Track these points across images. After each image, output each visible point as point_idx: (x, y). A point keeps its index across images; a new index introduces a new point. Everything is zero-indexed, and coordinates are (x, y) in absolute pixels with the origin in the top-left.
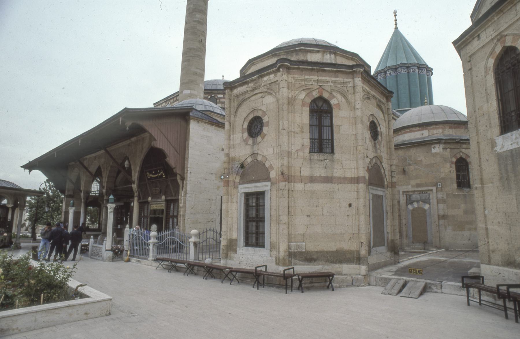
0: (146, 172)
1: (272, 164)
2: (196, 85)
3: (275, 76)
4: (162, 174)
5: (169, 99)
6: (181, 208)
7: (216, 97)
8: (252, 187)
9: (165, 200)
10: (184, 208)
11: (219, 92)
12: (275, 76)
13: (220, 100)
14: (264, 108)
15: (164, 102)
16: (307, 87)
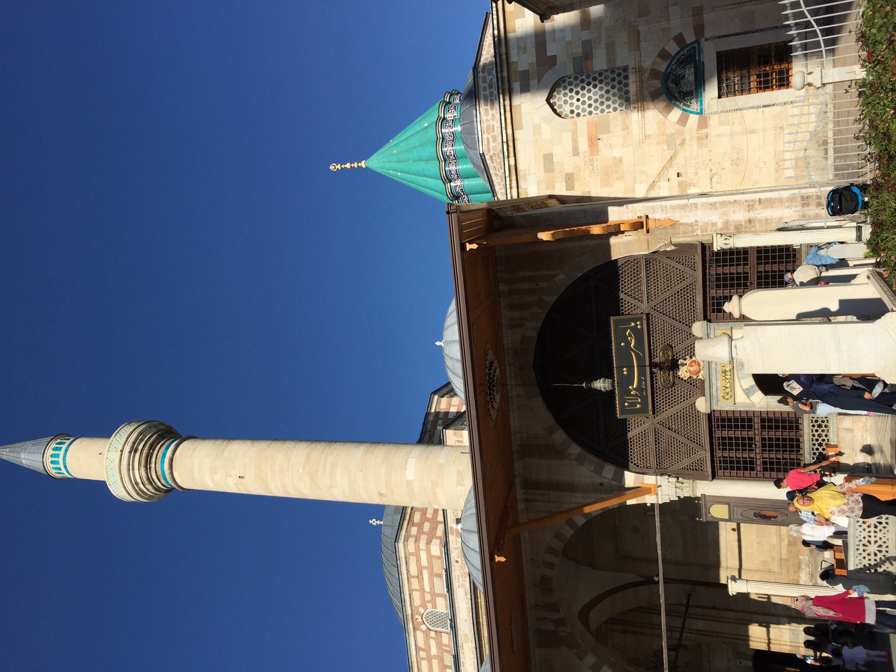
4: (631, 328)
6: (726, 223)
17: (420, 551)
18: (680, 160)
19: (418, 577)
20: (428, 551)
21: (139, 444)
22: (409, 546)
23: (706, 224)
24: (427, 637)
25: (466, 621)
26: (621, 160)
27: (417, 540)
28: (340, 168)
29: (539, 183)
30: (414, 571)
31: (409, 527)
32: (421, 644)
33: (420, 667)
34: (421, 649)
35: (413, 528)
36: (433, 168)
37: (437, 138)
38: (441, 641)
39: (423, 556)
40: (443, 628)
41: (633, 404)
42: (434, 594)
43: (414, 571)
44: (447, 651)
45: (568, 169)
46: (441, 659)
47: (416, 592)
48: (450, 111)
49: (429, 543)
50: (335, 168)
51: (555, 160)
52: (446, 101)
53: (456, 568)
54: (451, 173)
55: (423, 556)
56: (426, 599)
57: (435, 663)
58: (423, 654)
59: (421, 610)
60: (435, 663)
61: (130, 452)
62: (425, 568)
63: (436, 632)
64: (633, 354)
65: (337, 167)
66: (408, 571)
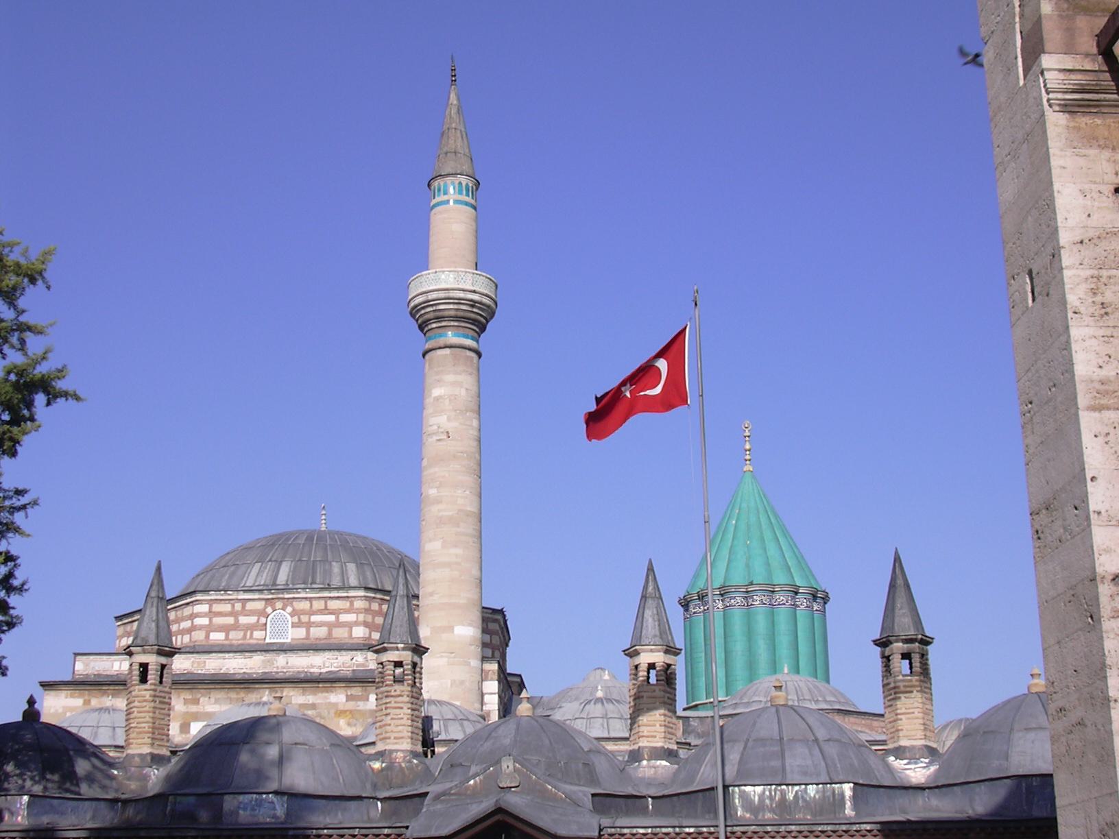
5: (287, 596)
17: (355, 615)
19: (326, 608)
20: (356, 624)
21: (479, 308)
22: (359, 601)
25: (287, 663)
27: (367, 611)
28: (745, 434)
31: (378, 600)
32: (250, 606)
33: (223, 602)
34: (243, 607)
35: (377, 604)
36: (738, 579)
37: (774, 585)
38: (256, 630)
39: (351, 617)
40: (271, 633)
42: (309, 625)
43: (333, 605)
44: (245, 635)
46: (236, 627)
47: (309, 605)
48: (805, 601)
49: (366, 624)
50: (746, 428)
52: (817, 593)
53: (345, 657)
54: (731, 598)
55: (351, 617)
56: (302, 616)
57: (230, 620)
58: (238, 606)
59: (289, 609)
60: (230, 620)
61: (471, 300)
62: (337, 618)
63: (266, 624)
65: (747, 430)
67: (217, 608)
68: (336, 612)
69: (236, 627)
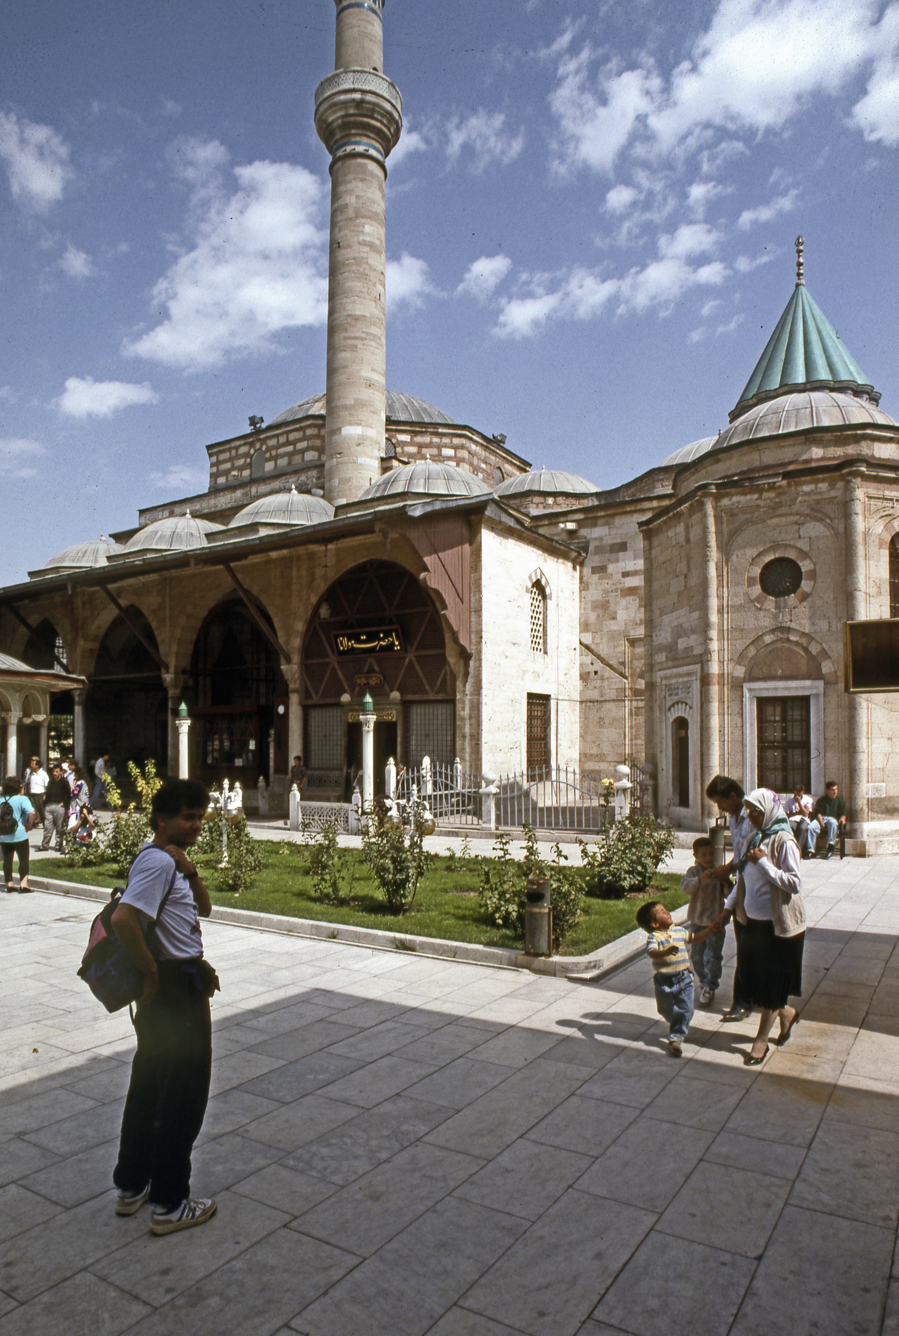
0: (337, 636)
1: (826, 648)
2: (374, 413)
3: (832, 486)
4: (393, 643)
6: (463, 719)
7: (394, 441)
8: (776, 689)
9: (401, 700)
10: (474, 722)
11: (509, 458)
12: (832, 486)
13: (402, 449)
14: (803, 545)
15: (245, 444)
16: (887, 513)
18: (608, 672)
20: (307, 449)
23: (464, 702)
24: (247, 455)
26: (614, 618)
29: (601, 539)
30: (292, 437)
41: (342, 644)
43: (292, 437)
45: (611, 568)
51: (621, 554)
55: (302, 445)
59: (264, 448)
60: (228, 465)
64: (376, 643)
66: (291, 431)
67: (222, 457)
68: (294, 443)
69: (233, 468)
